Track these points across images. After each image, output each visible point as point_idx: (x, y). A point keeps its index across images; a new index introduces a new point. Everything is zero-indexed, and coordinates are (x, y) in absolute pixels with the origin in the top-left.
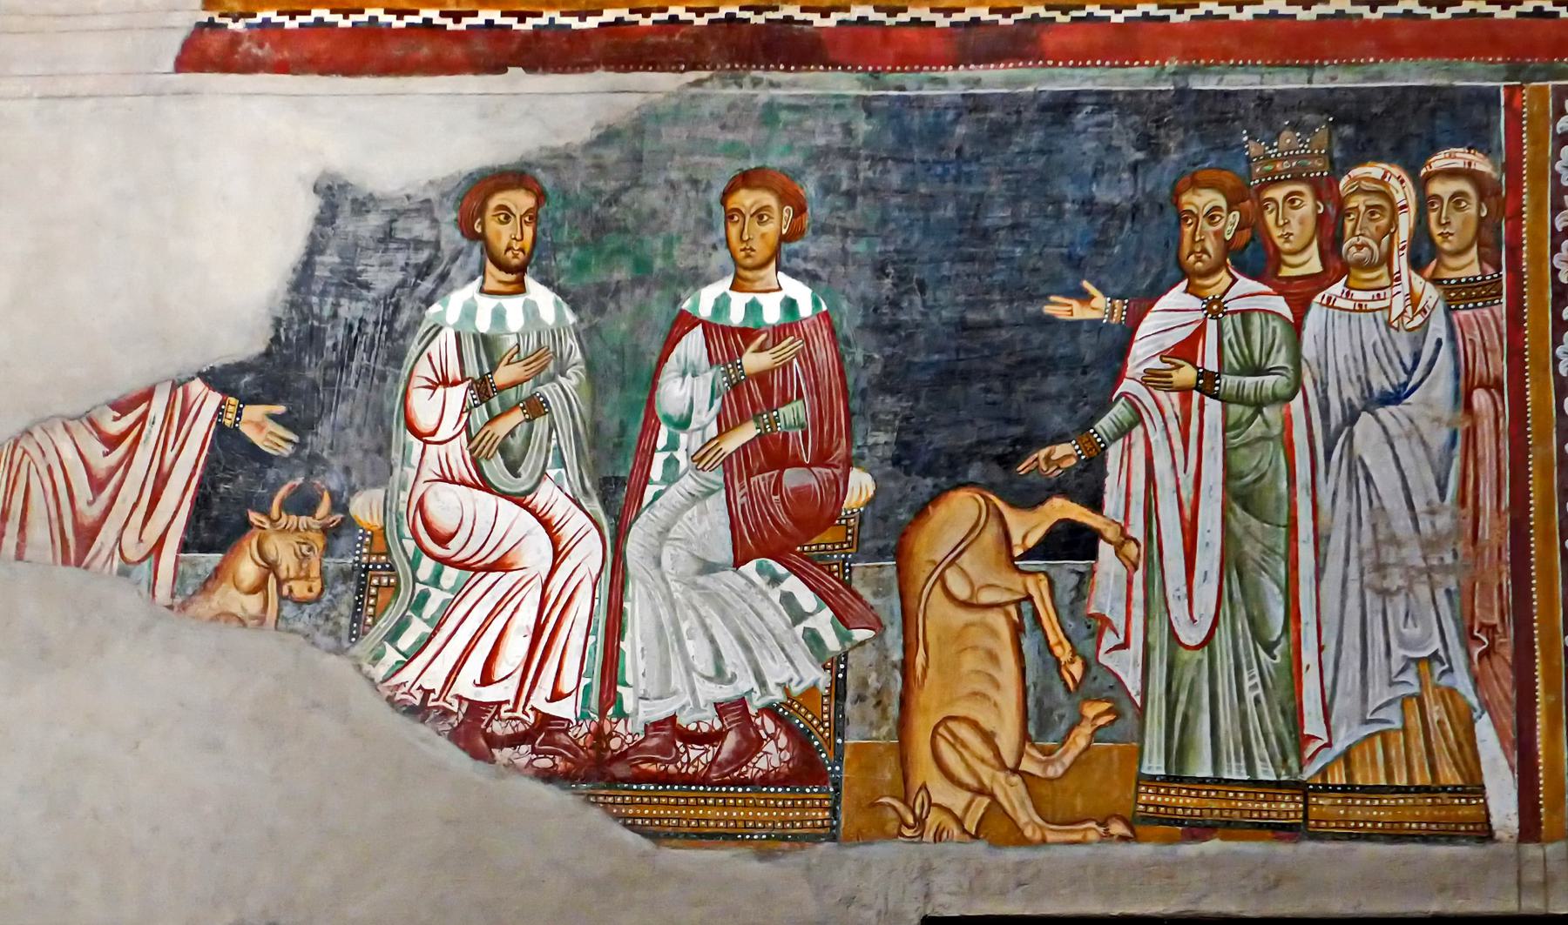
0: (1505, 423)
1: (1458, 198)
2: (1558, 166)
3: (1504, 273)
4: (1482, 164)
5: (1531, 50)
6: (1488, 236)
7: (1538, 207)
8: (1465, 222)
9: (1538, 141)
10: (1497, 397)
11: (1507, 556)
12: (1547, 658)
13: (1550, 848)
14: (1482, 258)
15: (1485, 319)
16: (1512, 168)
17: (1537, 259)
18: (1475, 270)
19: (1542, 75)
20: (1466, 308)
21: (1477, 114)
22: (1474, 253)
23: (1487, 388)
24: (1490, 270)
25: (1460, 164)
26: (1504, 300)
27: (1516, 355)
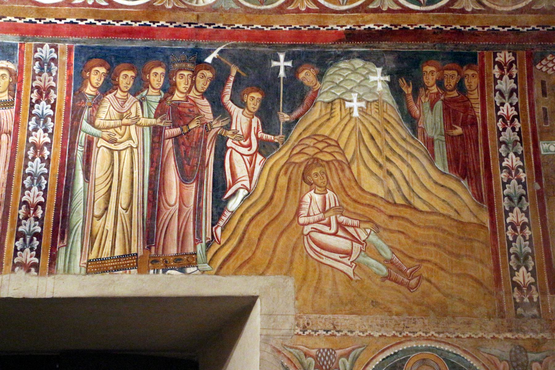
0: (10, 145)
1: (3, 76)
2: (35, 68)
3: (15, 99)
4: (11, 66)
5: (28, 32)
6: (12, 88)
7: (28, 80)
8: (5, 83)
9: (28, 59)
10: (9, 136)
11: (5, 185)
12: (13, 217)
13: (4, 276)
14: (9, 94)
15: (8, 113)
16: (21, 67)
17: (26, 95)
18: (6, 98)
19: (30, 40)
20: (3, 109)
21: (11, 51)
22: (7, 93)
23: (6, 134)
24: (11, 98)
25: (4, 66)
26: (14, 107)
27: (16, 123)
